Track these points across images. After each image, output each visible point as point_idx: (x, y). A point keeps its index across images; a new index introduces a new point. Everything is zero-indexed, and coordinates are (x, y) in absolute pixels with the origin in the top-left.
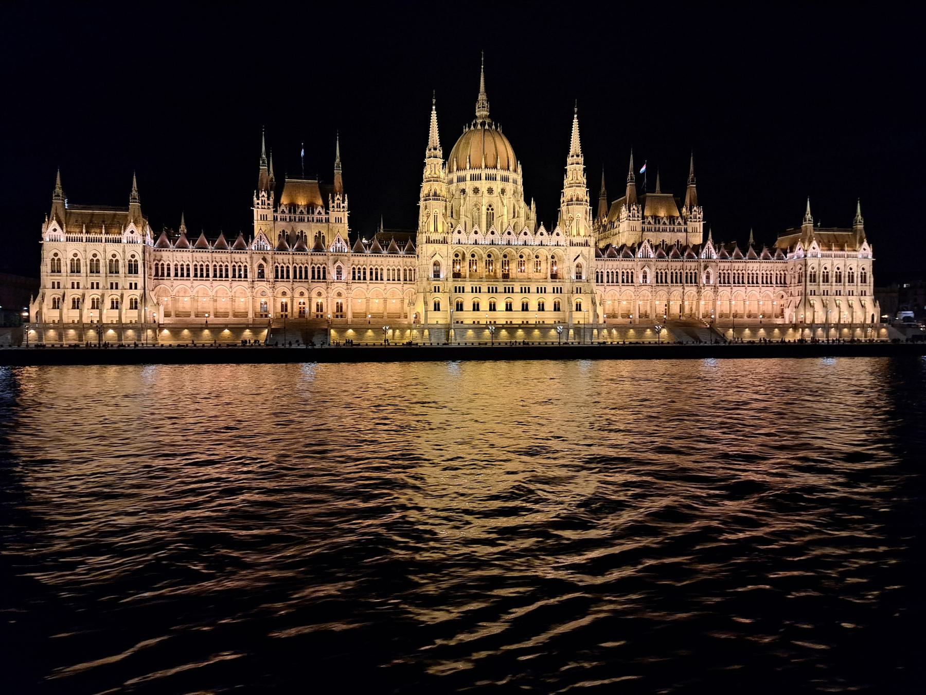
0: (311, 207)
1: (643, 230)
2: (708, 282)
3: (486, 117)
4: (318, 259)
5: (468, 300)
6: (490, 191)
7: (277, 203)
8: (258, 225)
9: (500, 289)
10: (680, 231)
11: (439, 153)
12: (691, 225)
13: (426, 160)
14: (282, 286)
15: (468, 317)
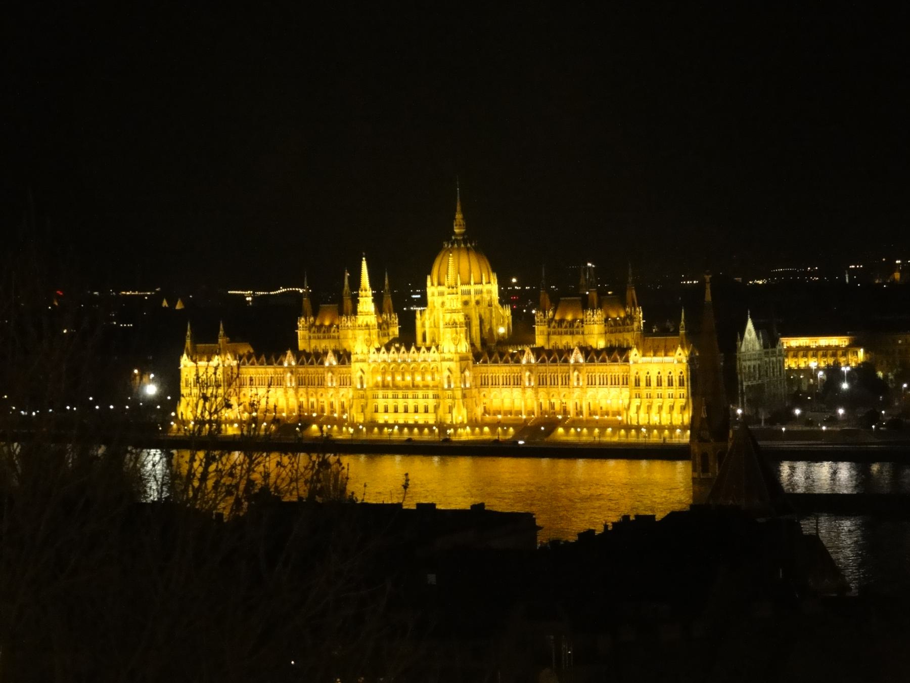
0: (331, 326)
1: (549, 334)
2: (578, 384)
3: (460, 234)
4: (320, 370)
5: (381, 403)
6: (443, 304)
7: (313, 325)
8: (302, 345)
9: (400, 396)
10: (578, 333)
11: (370, 293)
12: (587, 328)
13: (360, 299)
14: (302, 391)
15: (381, 418)
